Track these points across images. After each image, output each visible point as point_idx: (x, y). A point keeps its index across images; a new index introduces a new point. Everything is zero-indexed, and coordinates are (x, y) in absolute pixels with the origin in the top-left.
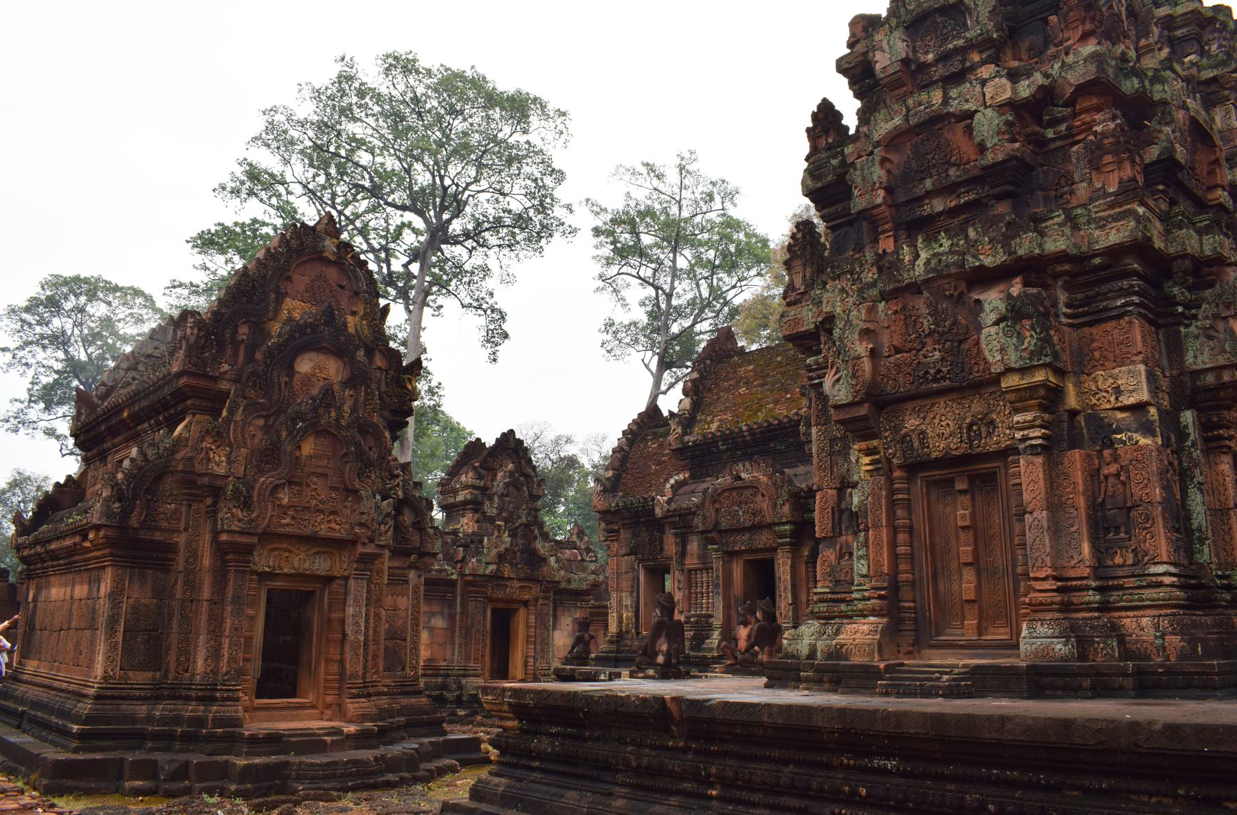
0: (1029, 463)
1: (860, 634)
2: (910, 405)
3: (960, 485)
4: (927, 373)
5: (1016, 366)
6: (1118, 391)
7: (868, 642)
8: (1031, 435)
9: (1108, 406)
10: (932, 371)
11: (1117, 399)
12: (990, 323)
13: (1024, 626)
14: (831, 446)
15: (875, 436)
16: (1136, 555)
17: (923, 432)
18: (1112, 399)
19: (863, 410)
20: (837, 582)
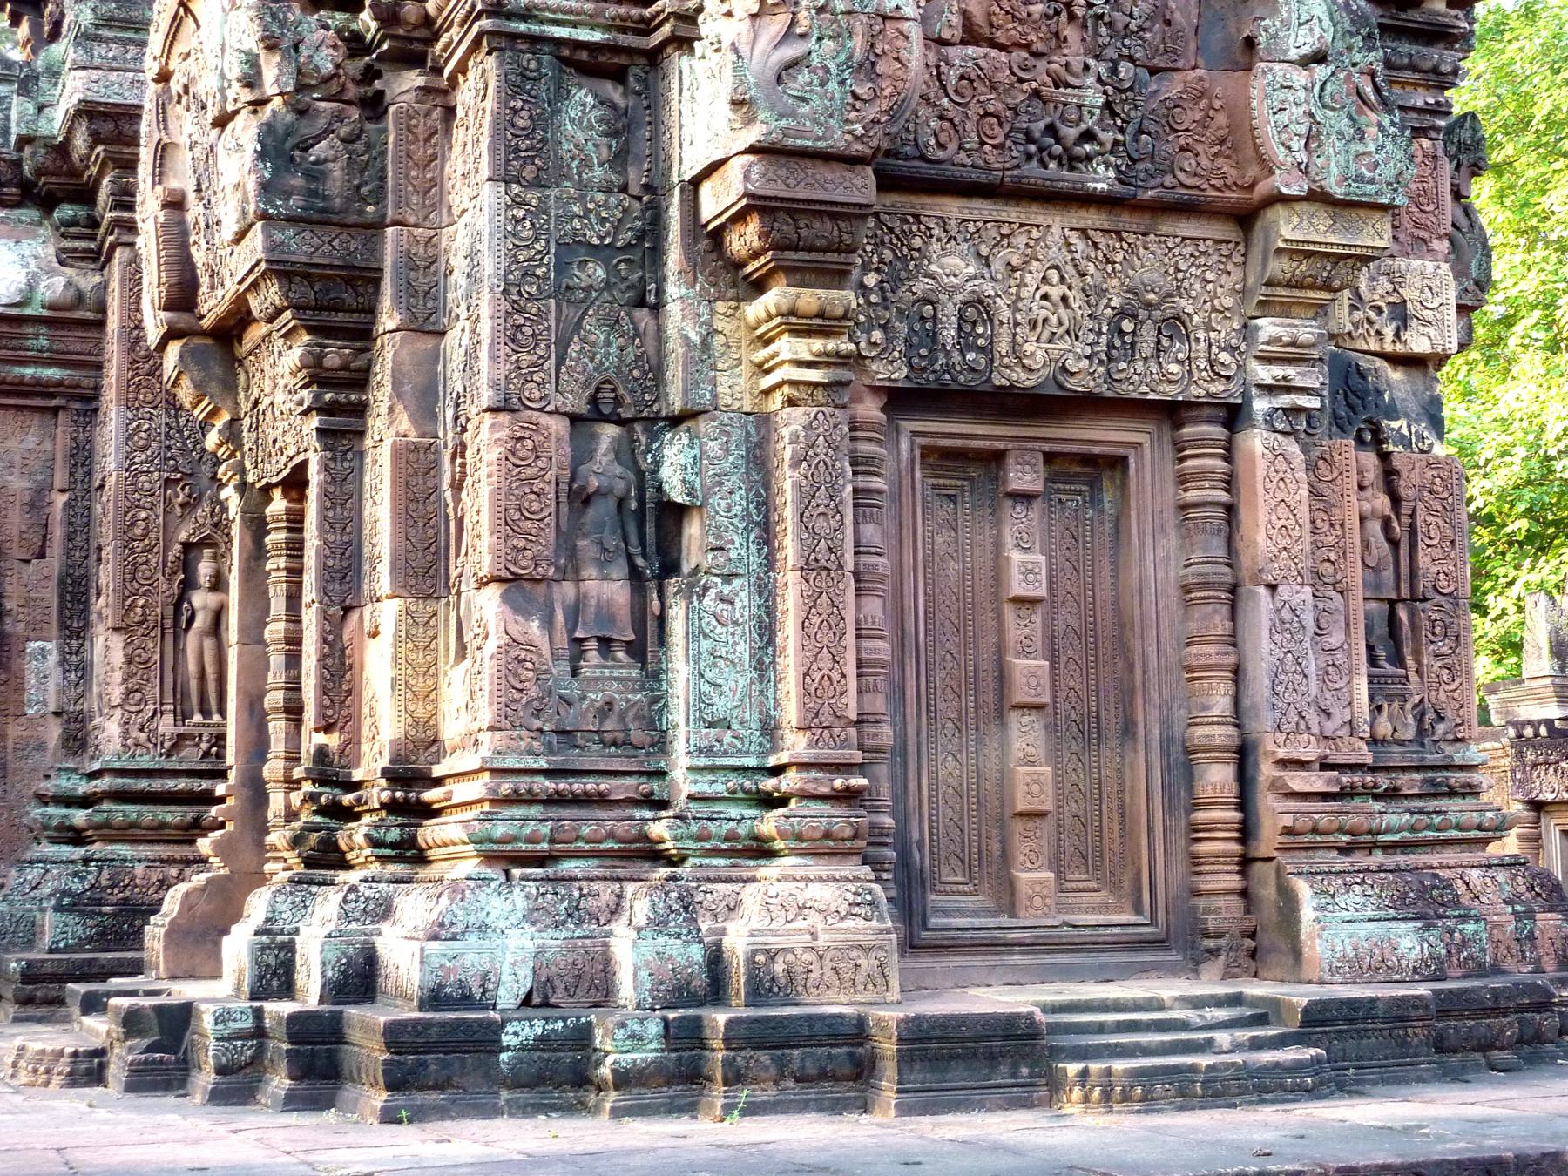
0: (1277, 454)
1: (798, 915)
2: (953, 208)
3: (1024, 476)
4: (1051, 130)
5: (1338, 192)
6: (1401, 315)
7: (868, 939)
8: (1299, 382)
9: (1373, 345)
10: (1071, 133)
11: (1397, 335)
12: (1293, 54)
13: (1303, 888)
14: (562, 267)
15: (837, 277)
16: (1420, 720)
17: (978, 302)
18: (1389, 331)
19: (860, 187)
20: (565, 734)
